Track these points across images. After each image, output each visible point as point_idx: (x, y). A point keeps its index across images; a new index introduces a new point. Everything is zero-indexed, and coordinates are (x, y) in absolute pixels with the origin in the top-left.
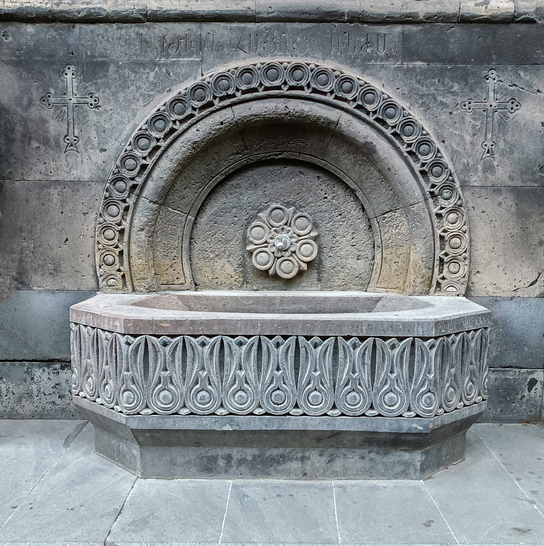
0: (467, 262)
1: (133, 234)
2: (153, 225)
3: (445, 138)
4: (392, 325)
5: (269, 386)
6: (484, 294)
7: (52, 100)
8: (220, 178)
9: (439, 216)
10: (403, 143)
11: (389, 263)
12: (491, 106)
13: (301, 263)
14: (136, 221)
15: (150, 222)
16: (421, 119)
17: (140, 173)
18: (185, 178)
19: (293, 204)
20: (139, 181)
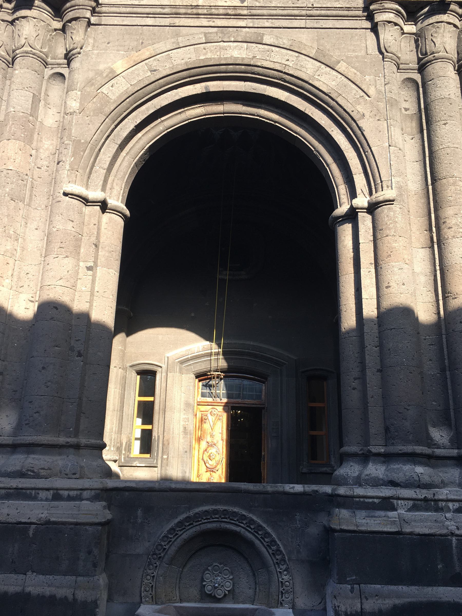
0: (292, 593)
6: (300, 608)
7: (132, 521)
8: (193, 552)
9: (280, 572)
20: (162, 555)
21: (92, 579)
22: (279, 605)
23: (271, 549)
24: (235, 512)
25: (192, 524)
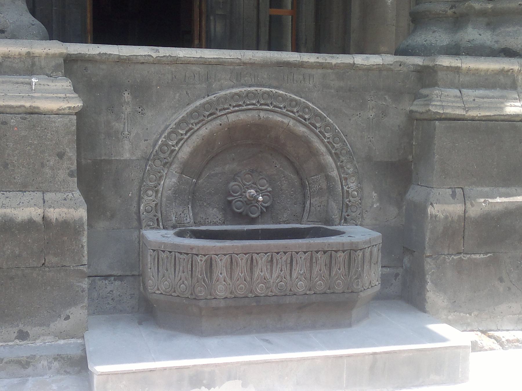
1: (164, 192)
12: (371, 115)
21: (70, 195)
22: (343, 221)
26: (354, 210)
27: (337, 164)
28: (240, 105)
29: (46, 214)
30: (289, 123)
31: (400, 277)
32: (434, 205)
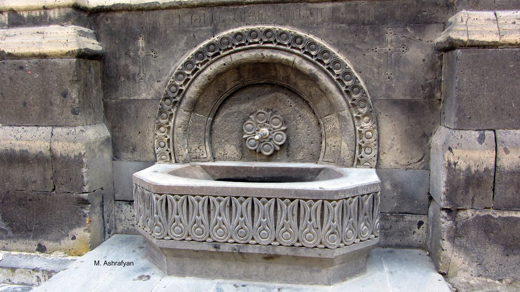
0: (376, 147)
1: (175, 129)
2: (186, 124)
3: (362, 70)
4: (310, 192)
5: (236, 226)
6: (388, 167)
8: (226, 95)
10: (334, 74)
11: (330, 146)
13: (275, 146)
14: (177, 122)
15: (185, 122)
16: (345, 59)
17: (179, 94)
18: (206, 96)
19: (272, 110)
20: (178, 99)
21: (73, 130)
22: (355, 163)
23: (343, 84)
24: (284, 33)
25: (218, 54)
26: (367, 151)
27: (348, 103)
28: (244, 45)
29: (52, 146)
30: (294, 61)
31: (424, 225)
32: (453, 150)
